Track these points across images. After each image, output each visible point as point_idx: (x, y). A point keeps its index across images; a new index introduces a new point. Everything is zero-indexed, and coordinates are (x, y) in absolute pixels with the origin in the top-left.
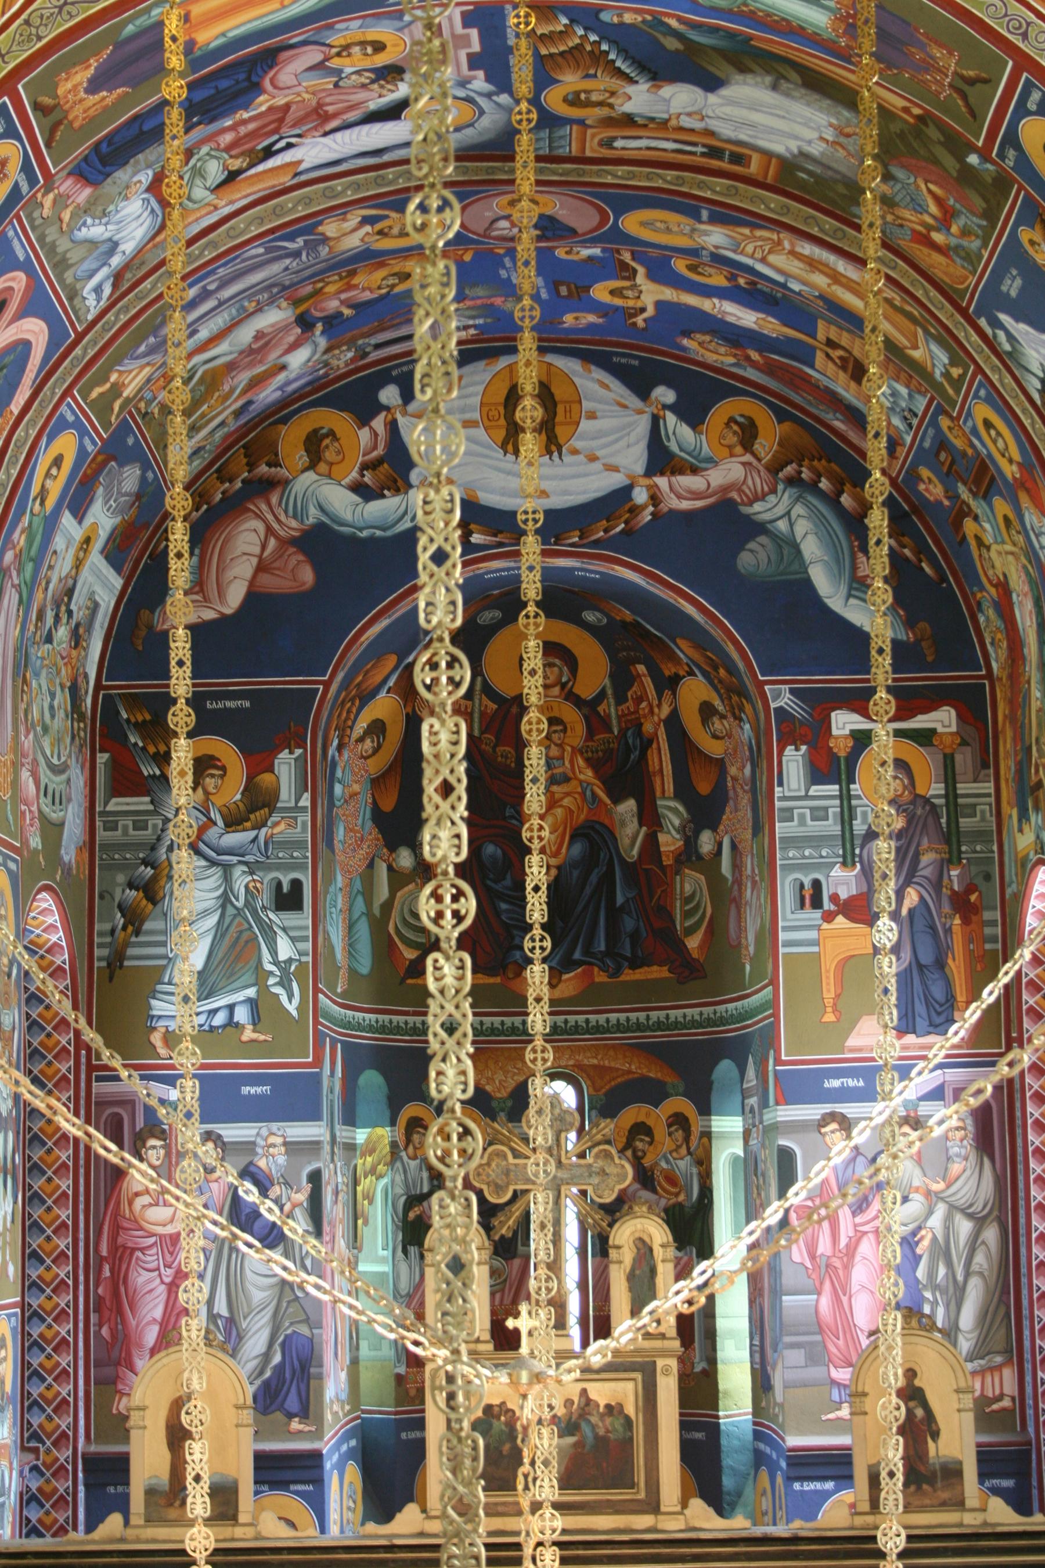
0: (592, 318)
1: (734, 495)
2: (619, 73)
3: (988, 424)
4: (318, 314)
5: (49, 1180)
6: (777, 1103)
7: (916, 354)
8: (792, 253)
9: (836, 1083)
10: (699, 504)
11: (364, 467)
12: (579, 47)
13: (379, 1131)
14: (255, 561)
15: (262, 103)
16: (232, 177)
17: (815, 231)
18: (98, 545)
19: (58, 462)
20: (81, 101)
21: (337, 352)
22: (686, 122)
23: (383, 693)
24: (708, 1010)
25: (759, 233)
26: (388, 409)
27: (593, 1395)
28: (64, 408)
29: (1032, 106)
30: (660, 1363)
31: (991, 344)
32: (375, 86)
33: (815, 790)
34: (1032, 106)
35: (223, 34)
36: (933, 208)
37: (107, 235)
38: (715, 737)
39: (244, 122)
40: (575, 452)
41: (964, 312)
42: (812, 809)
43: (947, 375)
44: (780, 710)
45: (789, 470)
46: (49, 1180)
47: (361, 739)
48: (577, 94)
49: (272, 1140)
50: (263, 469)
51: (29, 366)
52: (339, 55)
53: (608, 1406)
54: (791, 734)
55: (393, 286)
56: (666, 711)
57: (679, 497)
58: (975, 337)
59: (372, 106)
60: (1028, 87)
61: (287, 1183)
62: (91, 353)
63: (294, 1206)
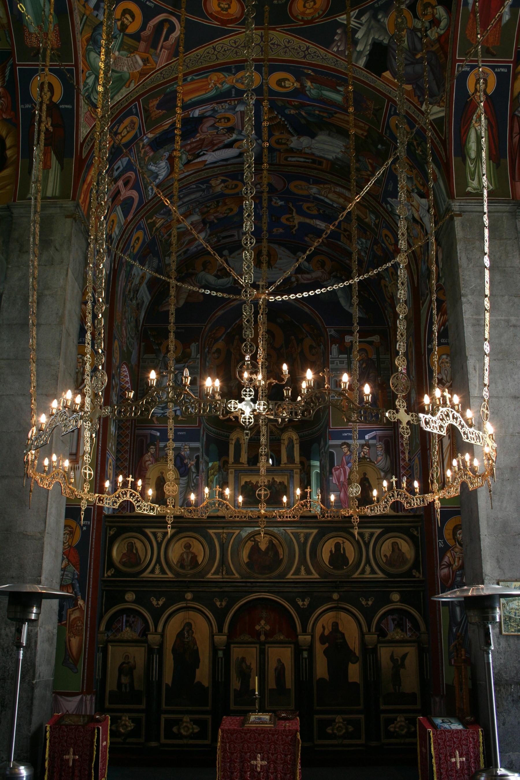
0: (281, 230)
1: (319, 280)
2: (289, 132)
3: (386, 236)
4: (208, 221)
5: (122, 454)
6: (329, 440)
7: (367, 220)
8: (335, 192)
9: (346, 434)
10: (309, 282)
11: (218, 271)
12: (279, 122)
13: (215, 463)
14: (187, 294)
15: (198, 137)
16: (189, 162)
17: (340, 183)
18: (146, 281)
19: (138, 239)
20: (155, 111)
21: (212, 237)
22: (307, 151)
23: (220, 341)
24: (310, 431)
25: (326, 186)
26: (225, 256)
27: (276, 479)
28: (141, 222)
29: (392, 113)
30: (295, 471)
31: (386, 210)
32: (227, 135)
33: (340, 356)
34: (392, 113)
35: (190, 100)
36: (370, 169)
37: (156, 171)
38: (313, 355)
39: (193, 143)
40: (276, 268)
41: (379, 202)
42: (340, 361)
43: (375, 224)
44: (331, 335)
45: (334, 273)
46: (122, 454)
47: (214, 353)
48: (278, 139)
49: (186, 447)
50: (191, 271)
51: (133, 208)
52: (218, 122)
53: (280, 482)
54: (334, 341)
55: (228, 213)
56: (300, 350)
57: (304, 280)
58: (382, 209)
59: (226, 142)
60: (391, 106)
61: (190, 459)
62: (149, 208)
63: (191, 465)
